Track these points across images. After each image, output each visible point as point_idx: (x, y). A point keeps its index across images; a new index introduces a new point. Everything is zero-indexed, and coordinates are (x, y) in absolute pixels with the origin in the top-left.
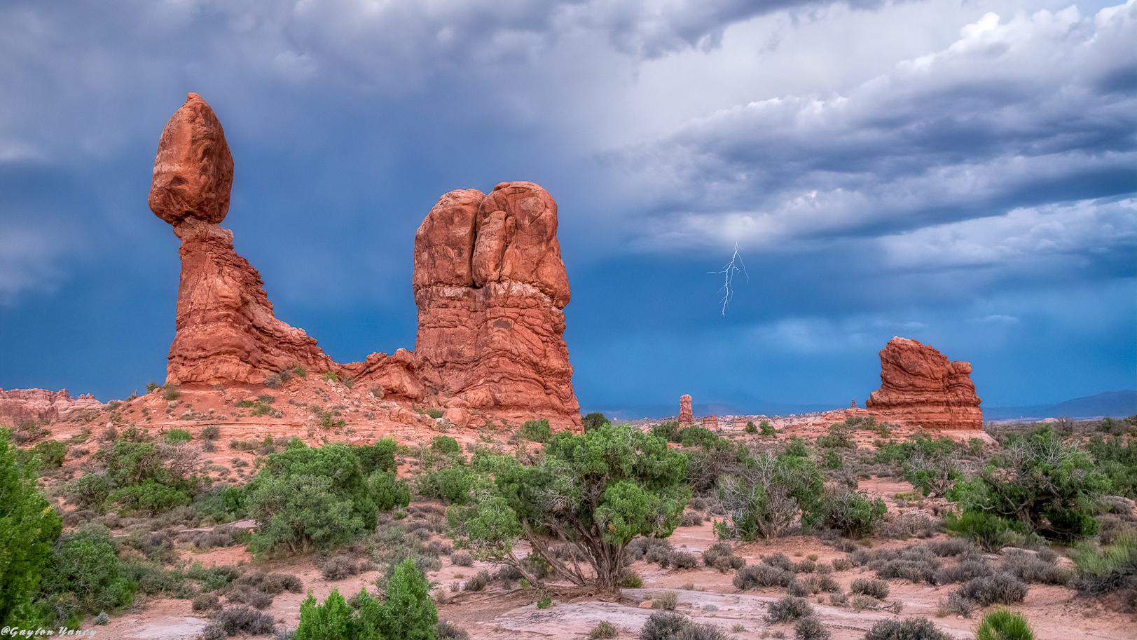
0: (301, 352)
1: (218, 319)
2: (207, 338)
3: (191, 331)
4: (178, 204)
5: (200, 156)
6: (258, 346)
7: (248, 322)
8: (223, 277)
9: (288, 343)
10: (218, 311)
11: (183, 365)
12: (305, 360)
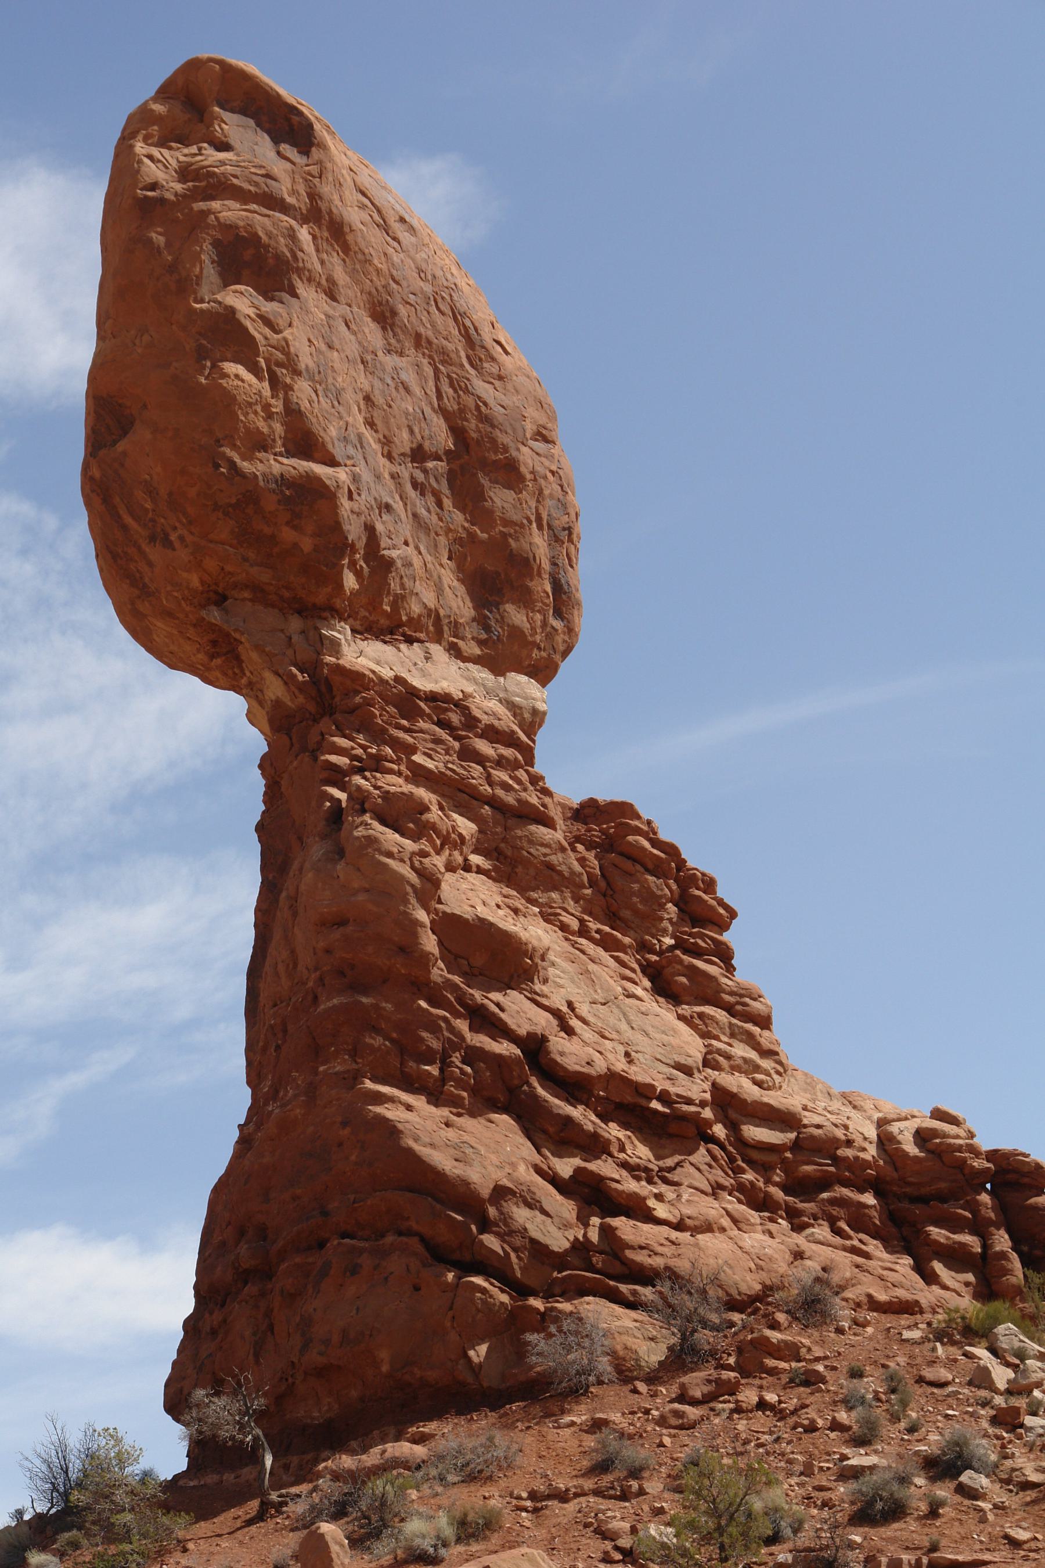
0: (937, 1233)
4: (152, 539)
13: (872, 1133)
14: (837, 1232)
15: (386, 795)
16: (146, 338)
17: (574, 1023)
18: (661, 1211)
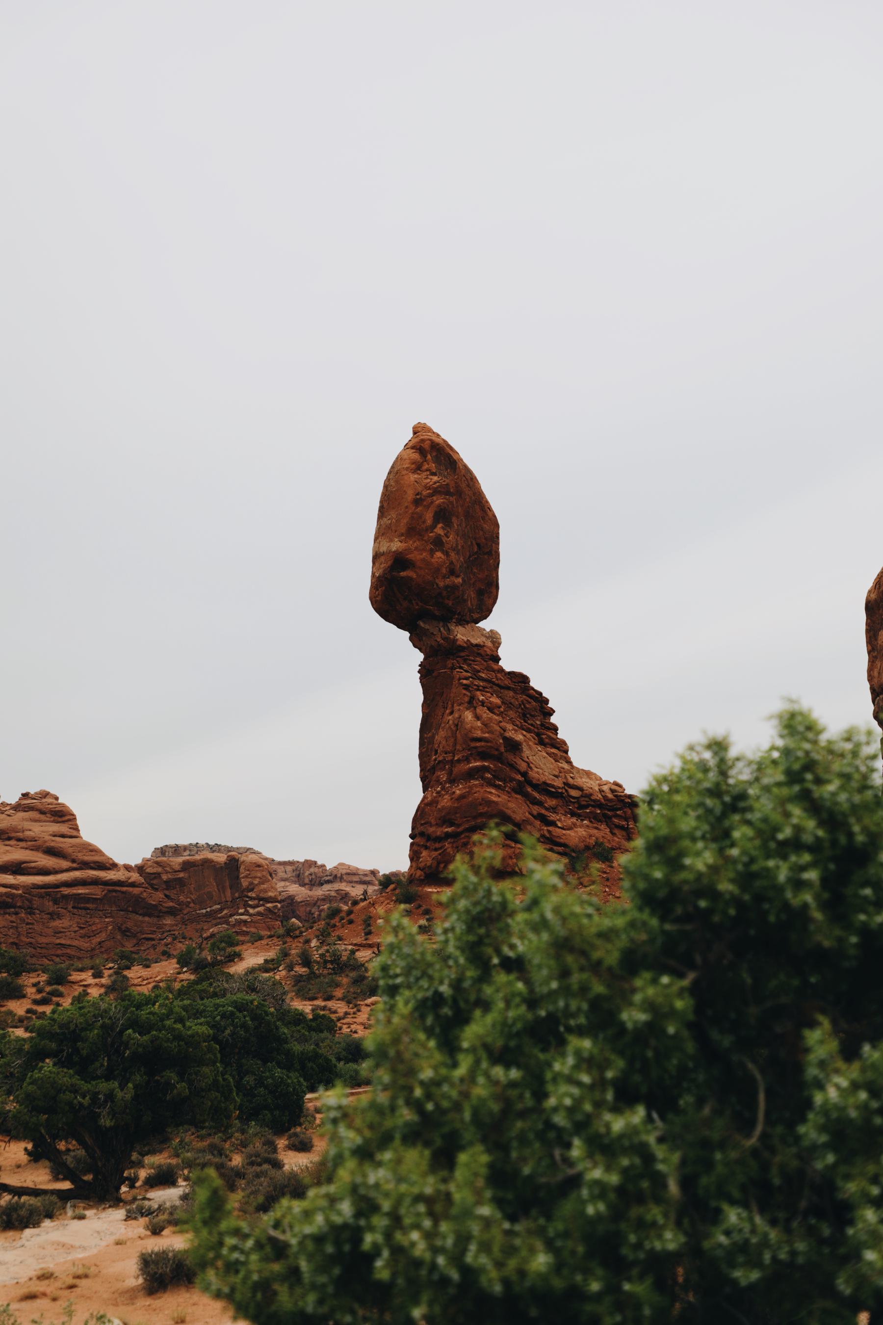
0: (616, 820)
1: (471, 774)
2: (456, 805)
3: (434, 794)
5: (429, 522)
6: (535, 813)
7: (519, 777)
8: (475, 708)
9: (593, 806)
10: (469, 763)
11: (426, 848)
12: (624, 833)
13: (597, 788)
14: (591, 822)
15: (491, 703)
16: (415, 544)
17: (531, 765)
18: (559, 825)
